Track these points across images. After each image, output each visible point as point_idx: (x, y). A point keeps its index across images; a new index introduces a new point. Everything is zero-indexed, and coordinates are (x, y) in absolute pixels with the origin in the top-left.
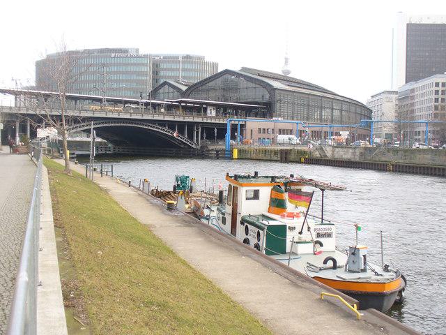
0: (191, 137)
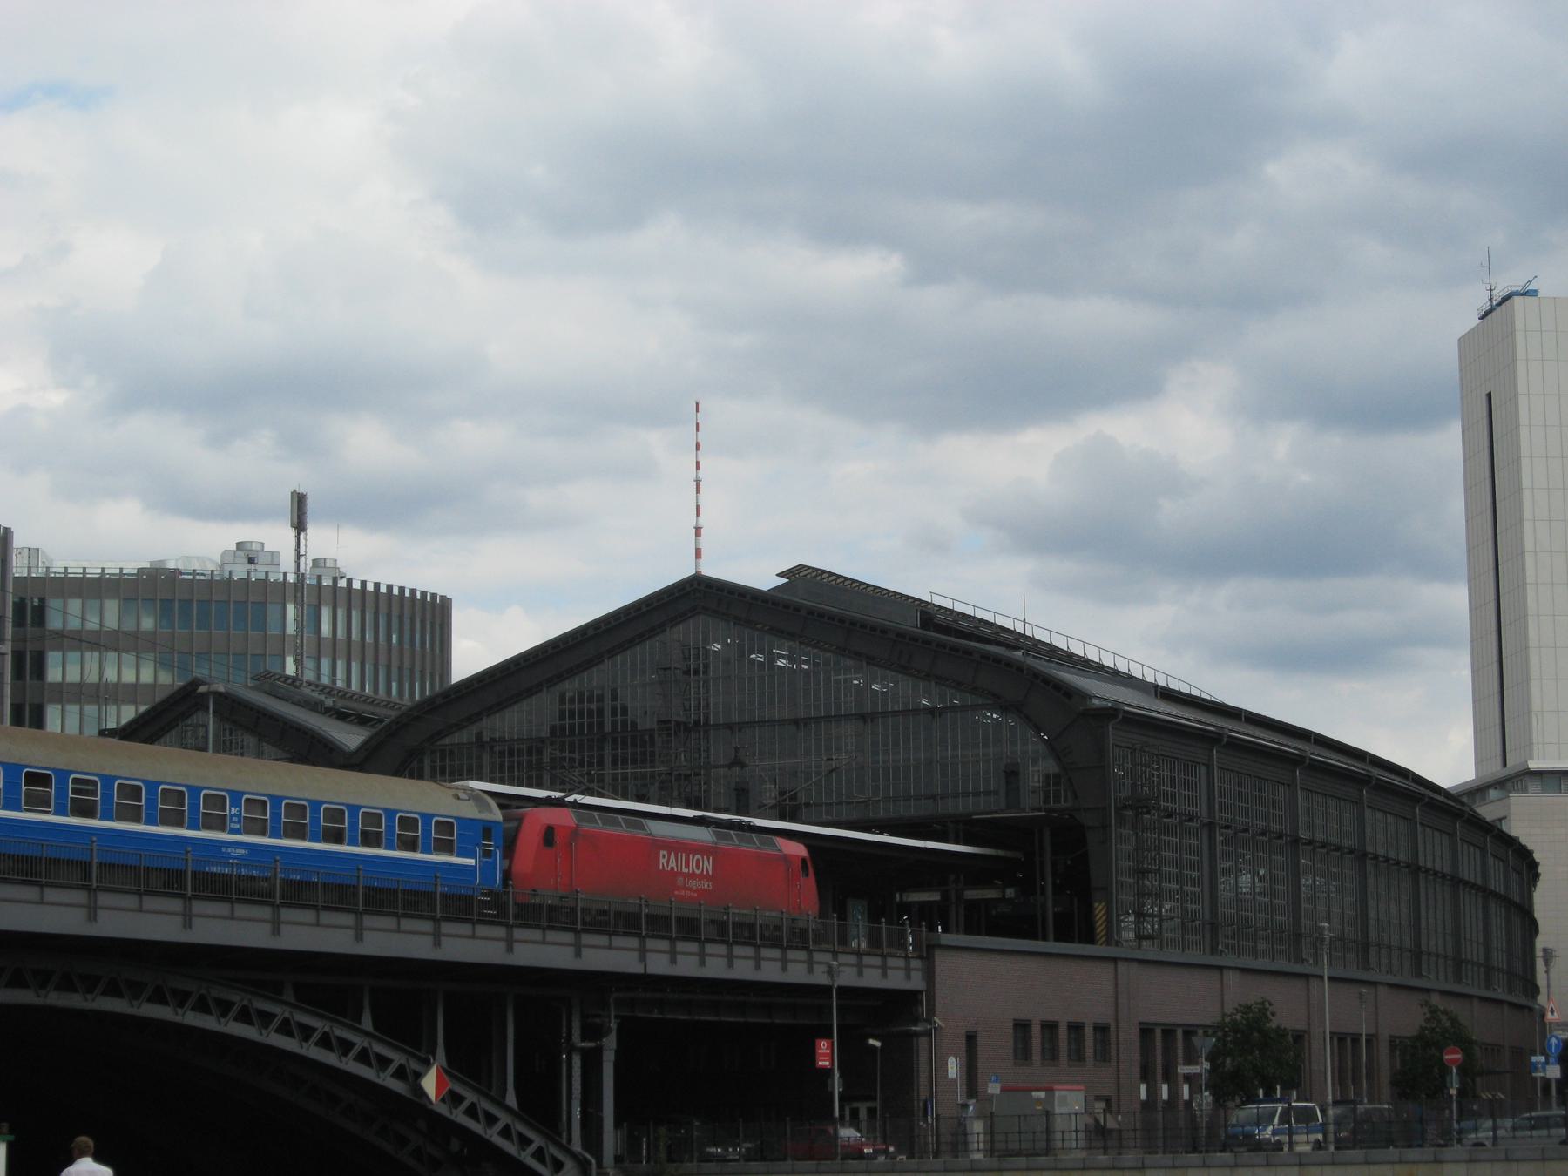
0: (540, 1105)
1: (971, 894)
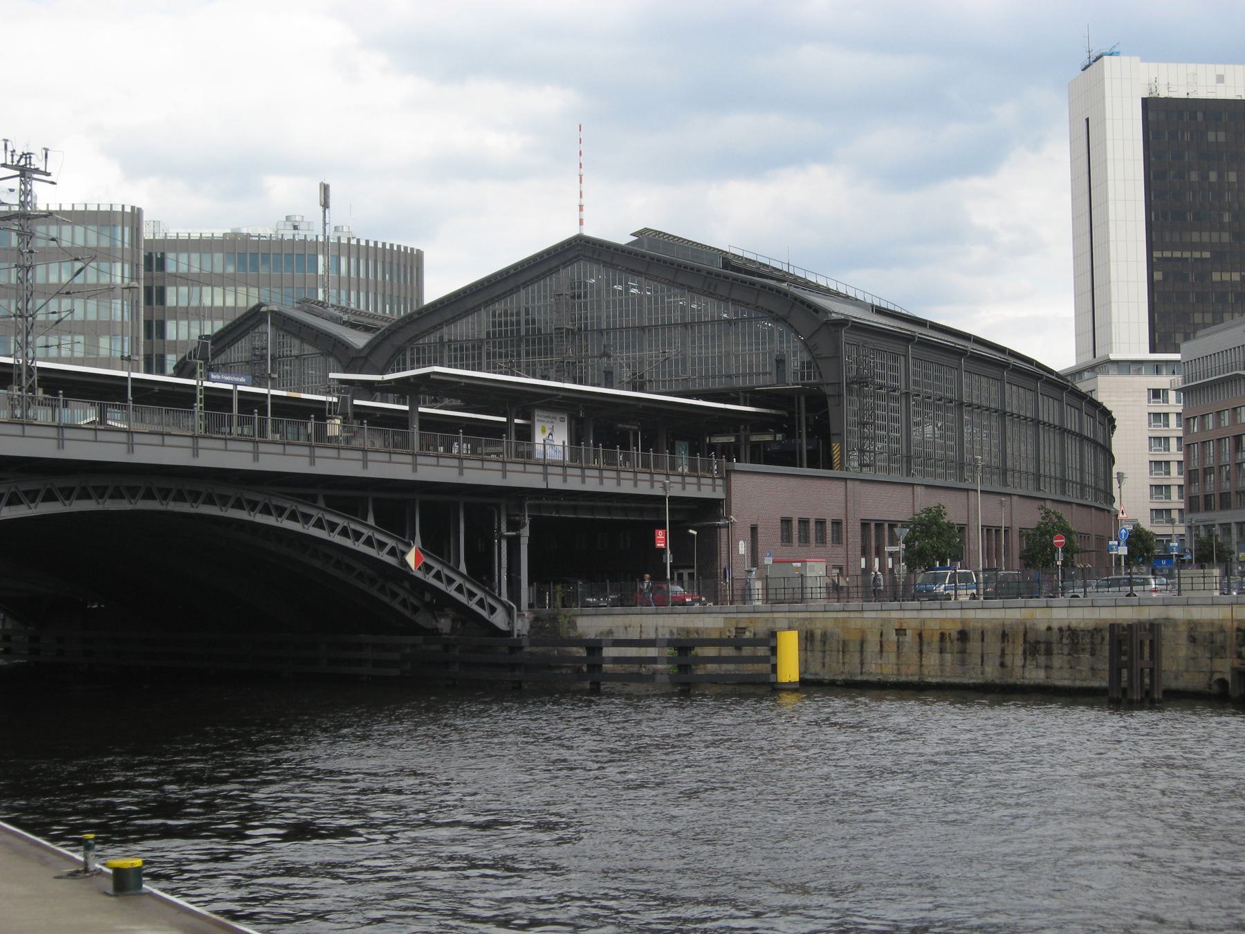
0: (481, 571)
1: (754, 438)
